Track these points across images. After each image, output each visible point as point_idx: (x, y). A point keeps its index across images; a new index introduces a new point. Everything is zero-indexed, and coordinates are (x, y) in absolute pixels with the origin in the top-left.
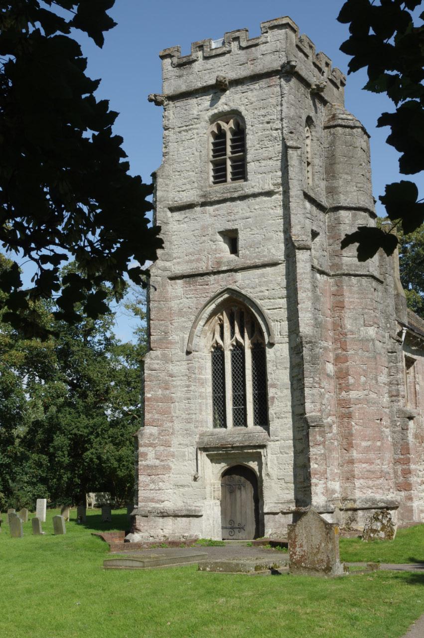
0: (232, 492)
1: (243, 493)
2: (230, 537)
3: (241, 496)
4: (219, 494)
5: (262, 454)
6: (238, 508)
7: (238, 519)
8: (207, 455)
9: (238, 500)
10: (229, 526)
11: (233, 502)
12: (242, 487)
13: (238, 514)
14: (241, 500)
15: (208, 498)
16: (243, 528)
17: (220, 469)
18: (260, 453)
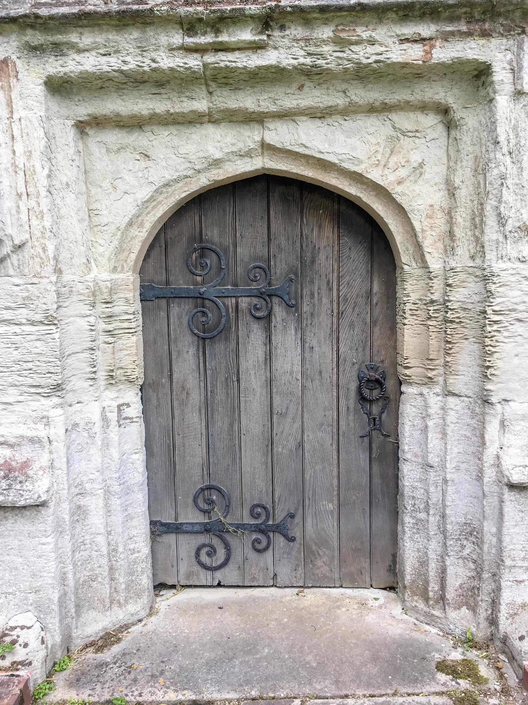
0: (212, 332)
1: (286, 340)
2: (205, 577)
3: (269, 357)
4: (130, 352)
5: (501, 75)
6: (253, 421)
7: (252, 478)
8: (59, 87)
9: (253, 380)
10: (192, 516)
11: (224, 391)
12: (279, 312)
13: (252, 460)
14: (270, 382)
15: (78, 383)
16: (280, 529)
17: (145, 193)
18: (479, 75)
